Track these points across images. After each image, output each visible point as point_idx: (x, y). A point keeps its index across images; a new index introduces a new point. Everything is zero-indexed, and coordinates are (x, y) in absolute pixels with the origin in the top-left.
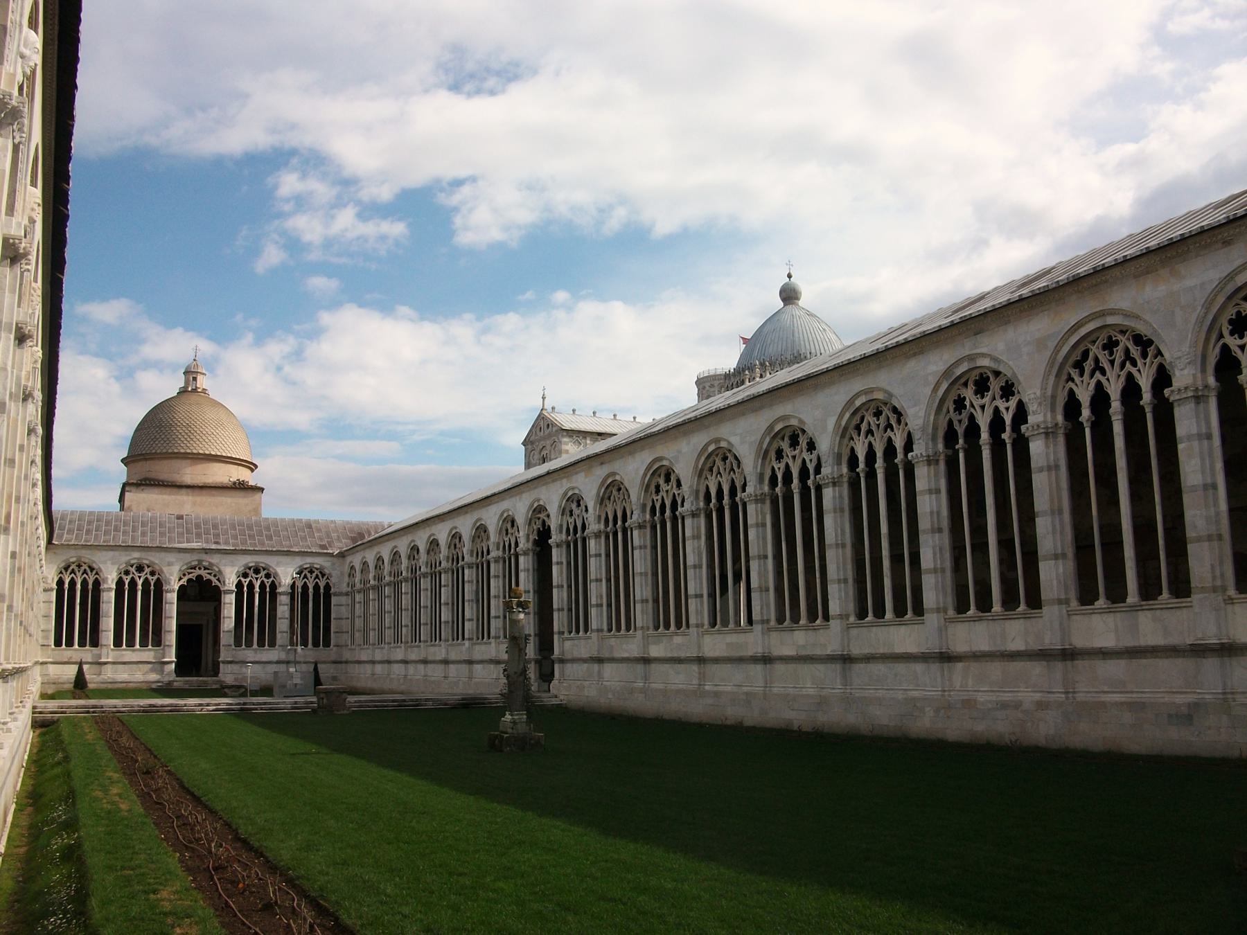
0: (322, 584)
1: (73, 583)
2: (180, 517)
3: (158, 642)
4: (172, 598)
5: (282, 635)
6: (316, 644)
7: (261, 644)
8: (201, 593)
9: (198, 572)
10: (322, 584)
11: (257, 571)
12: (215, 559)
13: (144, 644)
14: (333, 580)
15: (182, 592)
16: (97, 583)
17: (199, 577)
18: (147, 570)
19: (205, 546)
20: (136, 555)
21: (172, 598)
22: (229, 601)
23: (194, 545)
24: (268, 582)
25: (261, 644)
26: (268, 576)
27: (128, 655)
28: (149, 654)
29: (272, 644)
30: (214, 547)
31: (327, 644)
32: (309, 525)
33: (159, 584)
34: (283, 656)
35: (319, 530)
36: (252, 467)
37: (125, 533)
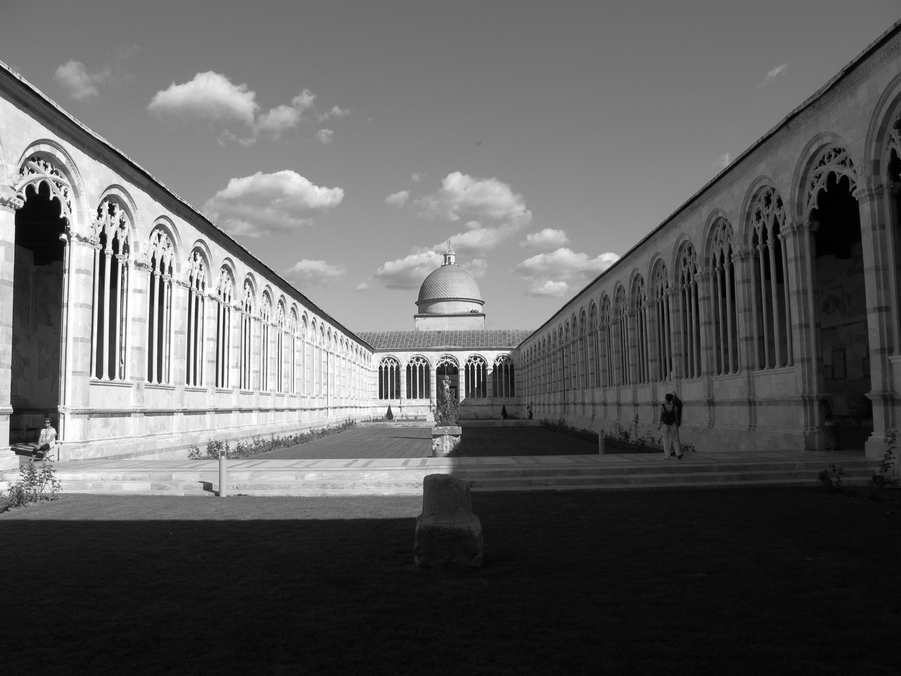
0: (509, 365)
1: (386, 368)
2: (439, 332)
3: (428, 396)
4: (433, 373)
5: (489, 392)
6: (507, 396)
7: (479, 396)
8: (448, 371)
9: (445, 360)
10: (509, 365)
11: (475, 358)
12: (454, 353)
13: (421, 397)
14: (515, 362)
15: (441, 371)
16: (398, 368)
17: (447, 362)
18: (421, 360)
19: (448, 347)
20: (416, 353)
21: (433, 373)
22: (462, 374)
23: (443, 347)
24: (481, 364)
25: (479, 396)
26: (481, 361)
27: (413, 402)
28: (425, 402)
29: (485, 396)
30: (453, 347)
31: (513, 395)
32: (504, 334)
33: (427, 367)
34: (490, 402)
35: (509, 336)
36: (482, 303)
37: (411, 342)
